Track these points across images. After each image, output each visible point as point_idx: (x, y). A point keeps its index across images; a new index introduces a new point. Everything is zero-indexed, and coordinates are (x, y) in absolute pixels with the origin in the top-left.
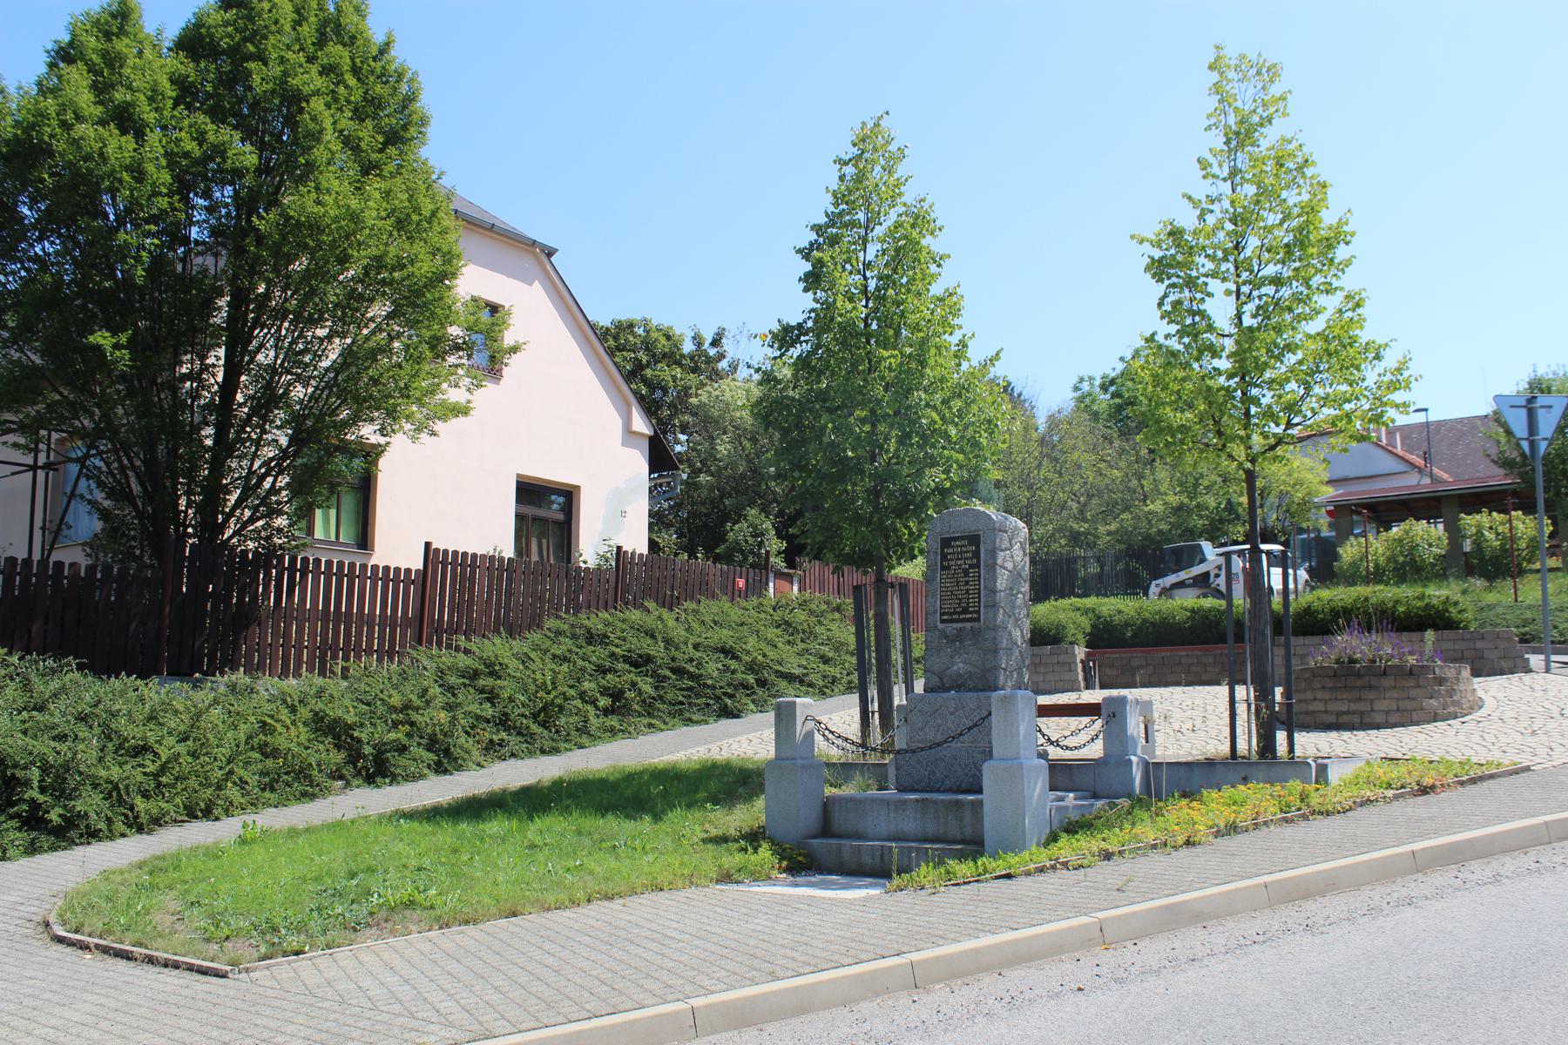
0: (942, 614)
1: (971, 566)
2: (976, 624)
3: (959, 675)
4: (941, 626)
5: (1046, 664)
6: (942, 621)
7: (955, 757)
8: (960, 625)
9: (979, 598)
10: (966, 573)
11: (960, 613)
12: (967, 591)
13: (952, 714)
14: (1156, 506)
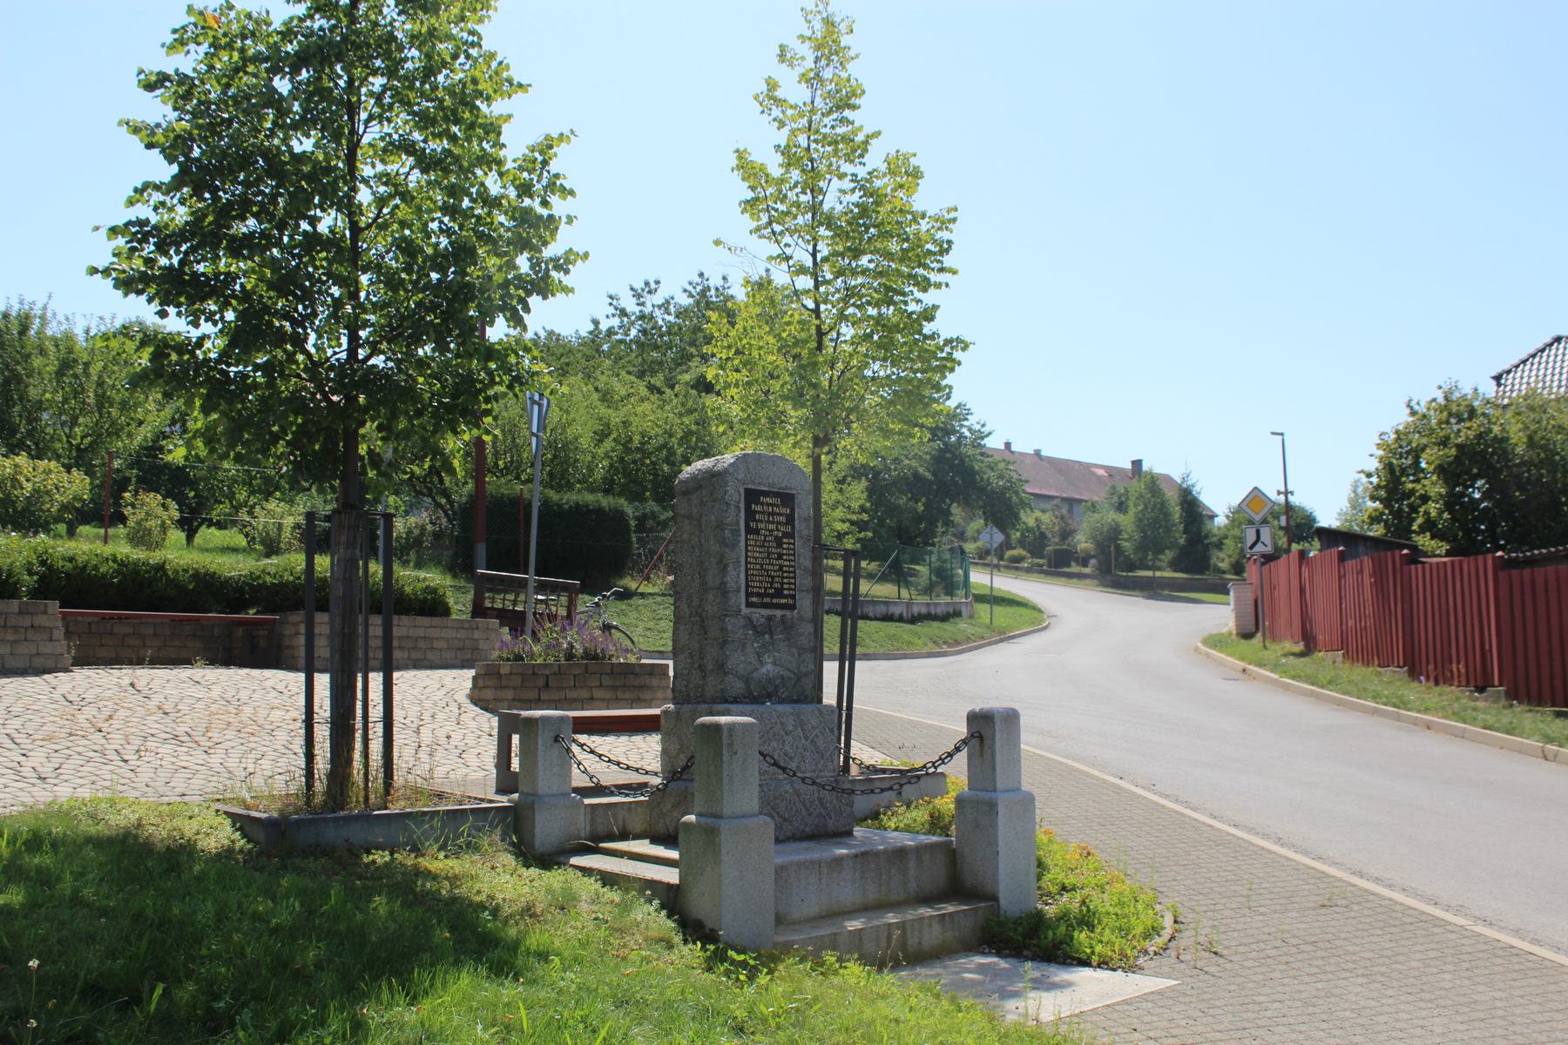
0: (748, 595)
1: (786, 535)
2: (787, 613)
3: (769, 681)
4: (745, 610)
5: (16, 629)
6: (749, 604)
10: (779, 544)
11: (772, 596)
12: (781, 567)
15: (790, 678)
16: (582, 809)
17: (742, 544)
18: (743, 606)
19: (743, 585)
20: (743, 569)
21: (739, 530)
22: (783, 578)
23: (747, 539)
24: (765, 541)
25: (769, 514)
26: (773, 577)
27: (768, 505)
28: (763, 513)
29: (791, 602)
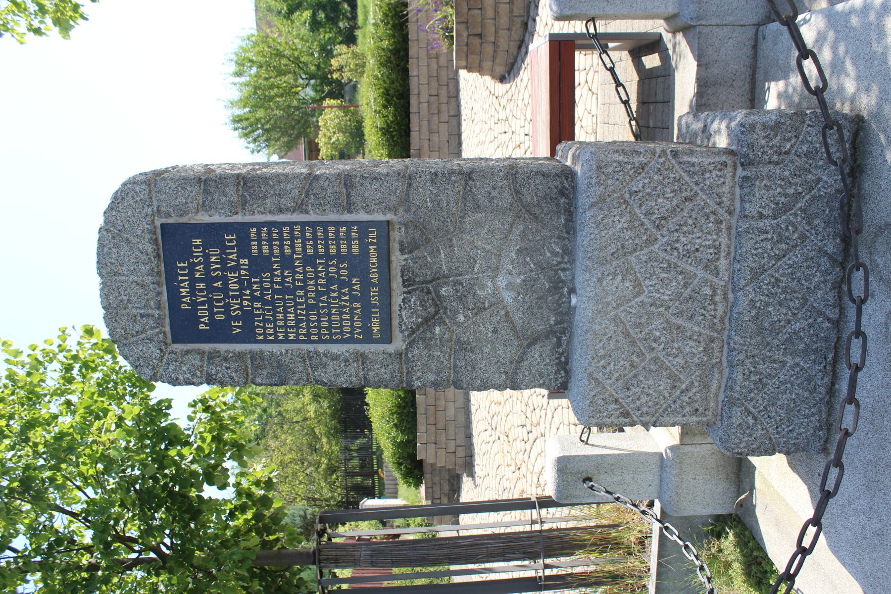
0: (368, 338)
1: (244, 251)
2: (396, 235)
3: (528, 285)
4: (398, 343)
6: (387, 338)
7: (757, 274)
8: (397, 284)
9: (325, 225)
10: (260, 265)
11: (366, 284)
13: (637, 284)
14: (311, 410)
15: (524, 235)
16: (687, 449)
17: (275, 348)
18: (391, 348)
19: (352, 347)
20: (321, 348)
21: (253, 356)
22: (328, 256)
23: (265, 341)
24: (260, 299)
25: (210, 289)
26: (330, 281)
27: (193, 291)
28: (210, 301)
29: (372, 236)
